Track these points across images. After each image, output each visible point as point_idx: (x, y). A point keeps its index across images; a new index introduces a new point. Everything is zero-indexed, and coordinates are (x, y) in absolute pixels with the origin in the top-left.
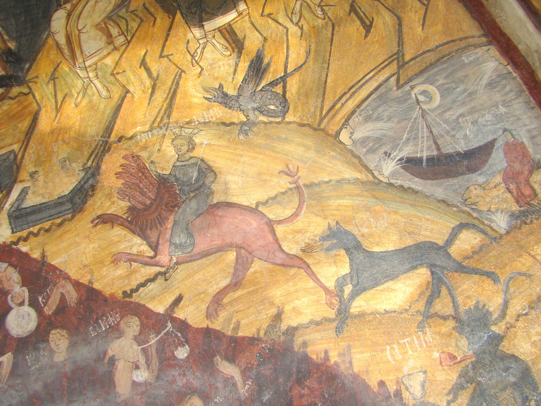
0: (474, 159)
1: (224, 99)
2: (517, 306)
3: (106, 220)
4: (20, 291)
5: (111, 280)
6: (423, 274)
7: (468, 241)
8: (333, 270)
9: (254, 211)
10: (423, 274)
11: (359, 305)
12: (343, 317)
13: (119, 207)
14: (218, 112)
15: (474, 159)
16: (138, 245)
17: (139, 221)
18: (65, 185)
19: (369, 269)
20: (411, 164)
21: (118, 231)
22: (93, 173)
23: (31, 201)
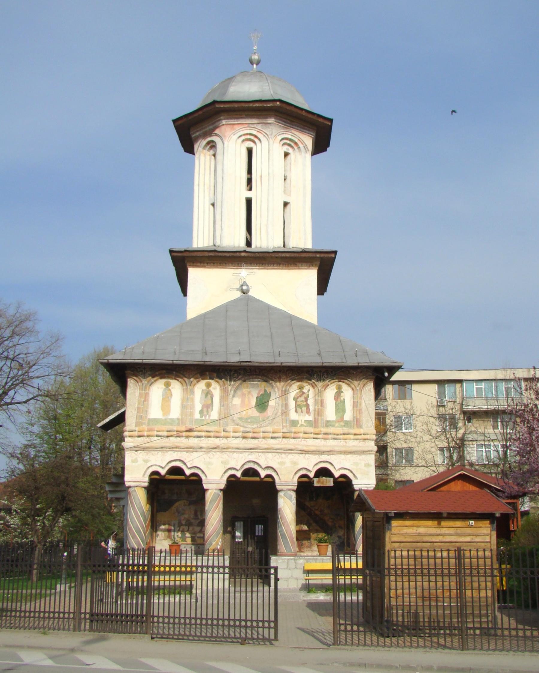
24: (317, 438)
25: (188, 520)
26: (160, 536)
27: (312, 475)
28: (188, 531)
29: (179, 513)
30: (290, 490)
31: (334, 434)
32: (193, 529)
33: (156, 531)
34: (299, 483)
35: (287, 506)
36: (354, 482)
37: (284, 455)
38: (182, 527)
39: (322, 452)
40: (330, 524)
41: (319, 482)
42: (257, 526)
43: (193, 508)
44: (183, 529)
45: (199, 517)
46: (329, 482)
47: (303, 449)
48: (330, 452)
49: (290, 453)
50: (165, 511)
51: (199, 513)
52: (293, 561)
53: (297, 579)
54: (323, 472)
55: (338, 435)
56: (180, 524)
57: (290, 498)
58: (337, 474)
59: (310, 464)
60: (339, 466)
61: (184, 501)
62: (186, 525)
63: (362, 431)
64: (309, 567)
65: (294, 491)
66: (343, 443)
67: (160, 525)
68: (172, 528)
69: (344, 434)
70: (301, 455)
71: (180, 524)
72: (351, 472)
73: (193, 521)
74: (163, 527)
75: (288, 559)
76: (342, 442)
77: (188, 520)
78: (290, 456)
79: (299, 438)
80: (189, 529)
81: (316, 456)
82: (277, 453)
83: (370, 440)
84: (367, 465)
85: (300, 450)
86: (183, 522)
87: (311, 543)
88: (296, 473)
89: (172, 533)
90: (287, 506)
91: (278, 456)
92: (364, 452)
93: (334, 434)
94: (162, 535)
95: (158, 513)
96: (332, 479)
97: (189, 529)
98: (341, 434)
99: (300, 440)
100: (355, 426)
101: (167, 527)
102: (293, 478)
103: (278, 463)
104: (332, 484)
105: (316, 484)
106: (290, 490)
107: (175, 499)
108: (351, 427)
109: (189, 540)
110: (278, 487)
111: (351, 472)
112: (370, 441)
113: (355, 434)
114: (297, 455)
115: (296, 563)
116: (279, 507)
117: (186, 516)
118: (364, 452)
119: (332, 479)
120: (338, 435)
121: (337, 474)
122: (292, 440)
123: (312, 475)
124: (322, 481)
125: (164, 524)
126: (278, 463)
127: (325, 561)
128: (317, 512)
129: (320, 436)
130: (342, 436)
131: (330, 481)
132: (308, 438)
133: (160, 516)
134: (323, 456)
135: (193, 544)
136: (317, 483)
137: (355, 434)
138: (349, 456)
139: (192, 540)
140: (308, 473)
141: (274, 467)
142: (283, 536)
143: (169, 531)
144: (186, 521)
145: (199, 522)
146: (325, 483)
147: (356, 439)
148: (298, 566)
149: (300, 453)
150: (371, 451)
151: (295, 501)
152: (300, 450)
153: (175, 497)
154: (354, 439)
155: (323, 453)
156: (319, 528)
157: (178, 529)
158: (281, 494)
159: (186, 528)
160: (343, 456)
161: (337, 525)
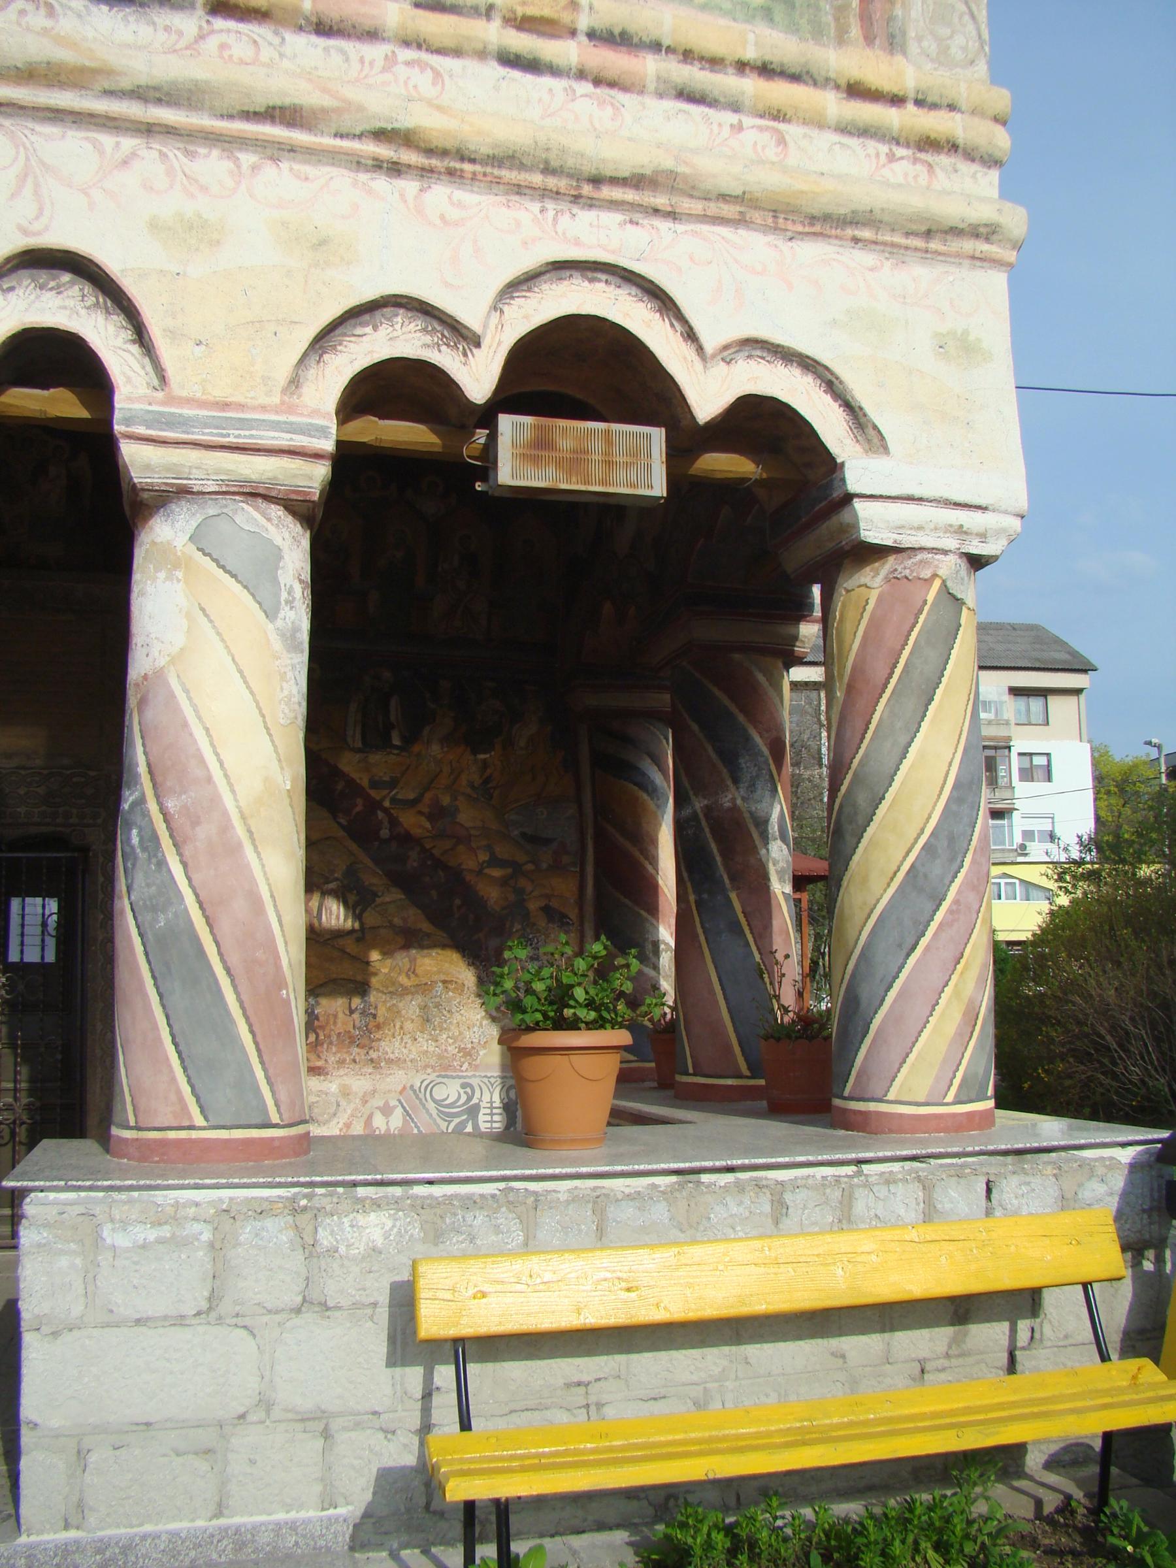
0: (547, 841)
1: (473, 787)
2: (535, 893)
3: (420, 813)
4: (386, 824)
5: (416, 832)
6: (510, 870)
7: (530, 867)
8: (483, 857)
9: (467, 829)
10: (510, 870)
11: (486, 871)
12: (480, 873)
13: (426, 810)
14: (469, 791)
15: (547, 841)
16: (428, 825)
17: (430, 817)
18: (412, 796)
19: (494, 862)
20: (523, 835)
21: (423, 818)
22: (422, 795)
23: (399, 797)
24: (531, 65)
27: (477, 376)
30: (256, 494)
31: (688, 56)
34: (349, 461)
35: (221, 658)
36: (859, 471)
37: (211, 164)
39: (576, 176)
40: (492, 895)
41: (540, 446)
42: (15, 904)
46: (631, 464)
47: (406, 121)
48: (646, 190)
49: (278, 151)
52: (278, 1231)
53: (321, 1424)
54: (584, 370)
55: (714, 63)
57: (257, 580)
58: (708, 394)
59: (476, 278)
60: (731, 319)
63: (900, 73)
64: (471, 1294)
65: (295, 506)
66: (755, 137)
69: (766, 70)
70: (382, 183)
72: (832, 385)
75: (227, 1212)
76: (750, 136)
78: (281, 180)
79: (372, 35)
81: (528, 211)
82: (149, 130)
83: (970, 155)
84: (959, 348)
85: (380, 135)
87: (369, 1014)
88: (325, 339)
90: (221, 658)
91: (150, 158)
92: (932, 235)
93: (688, 56)
96: (658, 435)
98: (742, 66)
99: (376, 52)
100: (855, 31)
102: (295, 382)
103: (154, 226)
104: (658, 488)
105: (509, 472)
106: (256, 494)
108: (818, 33)
110: (141, 461)
111: (832, 385)
112: (966, 168)
113: (856, 91)
114: (341, 179)
115: (310, 1249)
116: (140, 664)
118: (932, 235)
119: (658, 435)
120: (714, 63)
121: (708, 394)
122: (306, 48)
123: (477, 376)
124: (565, 444)
126: (154, 226)
127: (627, 1213)
128: (412, 822)
129: (566, 51)
130: (749, 86)
131: (638, 453)
132: (457, 52)
134: (586, 217)
136: (517, 457)
137: (856, 91)
138: (810, 251)
140: (447, 359)
141: (112, 262)
142: (178, 956)
146: (597, 471)
147: (865, 132)
148: (340, 1285)
149: (378, 165)
150: (985, 232)
151: (298, 616)
152: (380, 135)
154: (846, 129)
155: (587, 186)
156: (414, 917)
158: (164, 536)
160: (756, 246)
161: (533, 906)
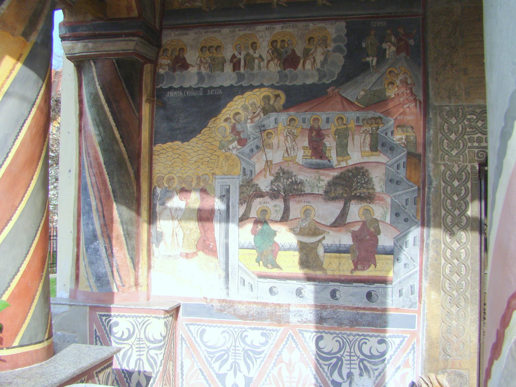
25: (282, 174)
26: (167, 237)
28: (284, 219)
29: (242, 142)
32: (307, 212)
33: (152, 219)
38: (257, 204)
43: (304, 116)
44: (264, 212)
45: (333, 155)
50: (187, 135)
51: (330, 143)
56: (250, 192)
61: (265, 92)
62: (274, 195)
67: (168, 194)
68: (219, 205)
71: (250, 192)
73: (305, 176)
74: (176, 202)
77: (282, 174)
80: (287, 210)
86: (264, 183)
89: (218, 227)
94: (174, 234)
95: (156, 148)
97: (287, 210)
101: (195, 200)
107: (227, 84)
109: (290, 262)
117: (276, 156)
125: (183, 191)
133: (169, 160)
135: (309, 279)
139: (304, 263)
143: (204, 216)
144: (277, 178)
145: (334, 184)
153: (227, 78)
157: (242, 210)
159: (275, 207)
